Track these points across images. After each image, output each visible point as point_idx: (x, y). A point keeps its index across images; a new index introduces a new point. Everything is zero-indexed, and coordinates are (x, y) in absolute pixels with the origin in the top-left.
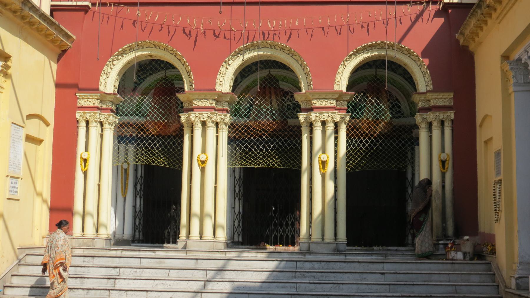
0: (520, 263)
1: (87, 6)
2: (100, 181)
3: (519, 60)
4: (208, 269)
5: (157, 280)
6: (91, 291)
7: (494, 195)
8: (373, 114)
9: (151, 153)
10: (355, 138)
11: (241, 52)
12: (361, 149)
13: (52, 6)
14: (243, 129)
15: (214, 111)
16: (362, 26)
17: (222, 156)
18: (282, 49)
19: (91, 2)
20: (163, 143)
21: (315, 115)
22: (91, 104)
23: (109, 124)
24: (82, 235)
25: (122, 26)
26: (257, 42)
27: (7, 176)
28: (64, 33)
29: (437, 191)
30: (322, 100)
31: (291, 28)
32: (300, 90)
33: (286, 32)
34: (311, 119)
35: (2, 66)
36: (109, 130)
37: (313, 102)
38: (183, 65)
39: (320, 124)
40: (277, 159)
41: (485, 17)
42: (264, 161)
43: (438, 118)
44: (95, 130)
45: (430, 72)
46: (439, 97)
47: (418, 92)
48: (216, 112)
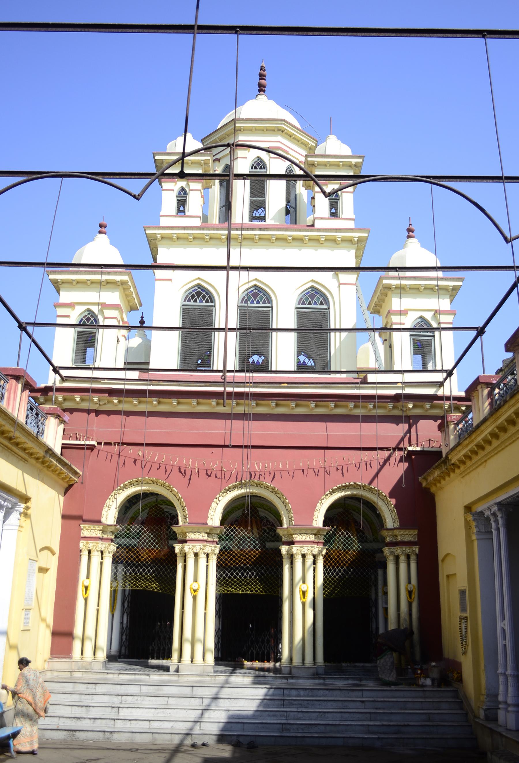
0: (488, 695)
1: (94, 446)
2: (98, 606)
3: (482, 513)
4: (204, 697)
5: (158, 708)
6: (97, 720)
7: (460, 629)
8: (342, 543)
9: (145, 578)
10: (329, 567)
11: (230, 490)
12: (335, 577)
13: (63, 444)
14: (229, 557)
15: (205, 544)
16: (337, 468)
17: (212, 584)
18: (267, 487)
19: (98, 441)
20: (156, 569)
21: (296, 548)
22: (94, 535)
23: (109, 552)
24: (80, 658)
25: (124, 463)
26: (245, 481)
27: (23, 610)
28: (73, 471)
29: (405, 620)
30: (303, 535)
31: (275, 470)
32: (281, 524)
33: (270, 473)
34: (293, 552)
35: (24, 508)
36: (108, 558)
37: (294, 536)
38: (178, 500)
39: (301, 556)
40: (259, 586)
41: (448, 471)
42: (248, 587)
43: (404, 552)
44: (96, 558)
45: (397, 511)
46: (405, 533)
47: (385, 527)
48: (208, 544)
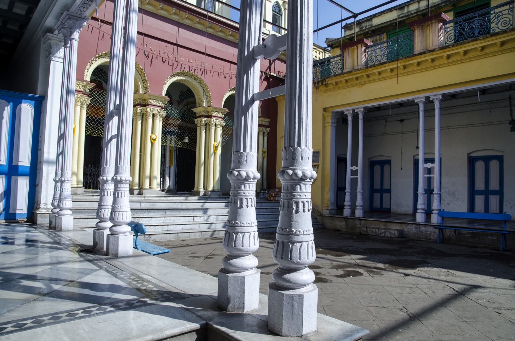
3: (342, 113)
11: (174, 75)
18: (197, 79)
23: (87, 104)
25: (103, 37)
26: (185, 71)
38: (140, 75)
39: (214, 125)
40: (179, 142)
